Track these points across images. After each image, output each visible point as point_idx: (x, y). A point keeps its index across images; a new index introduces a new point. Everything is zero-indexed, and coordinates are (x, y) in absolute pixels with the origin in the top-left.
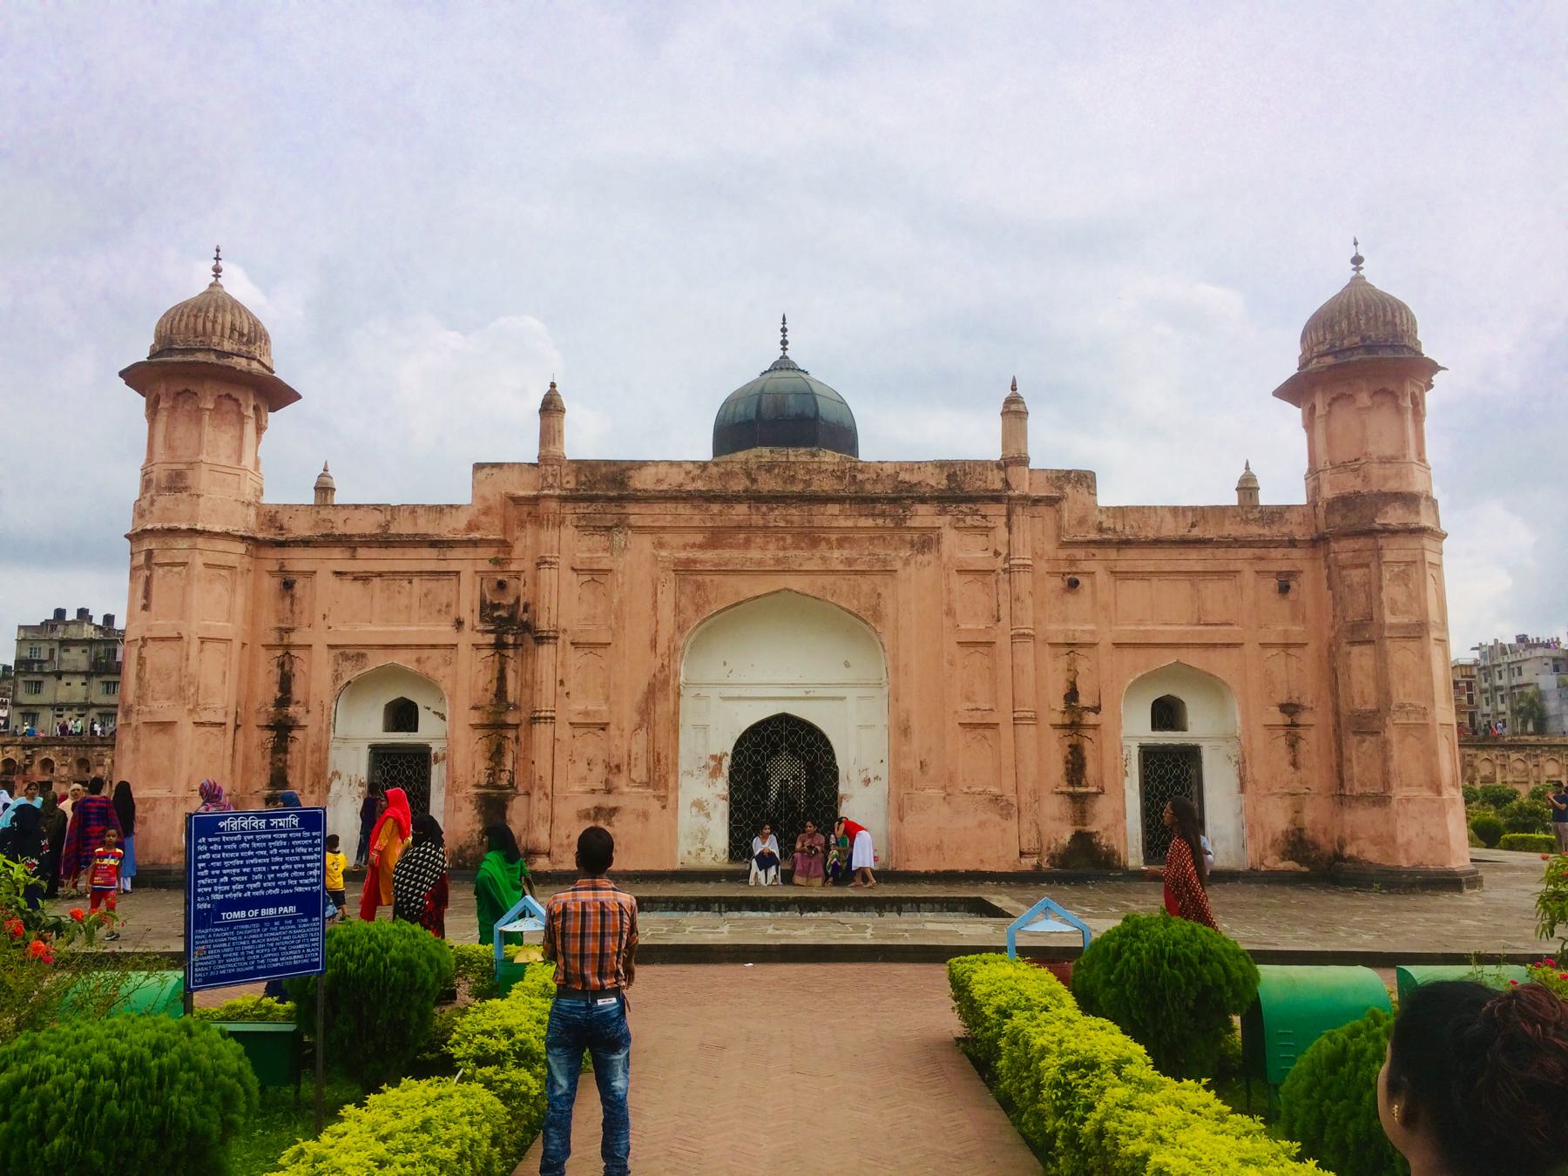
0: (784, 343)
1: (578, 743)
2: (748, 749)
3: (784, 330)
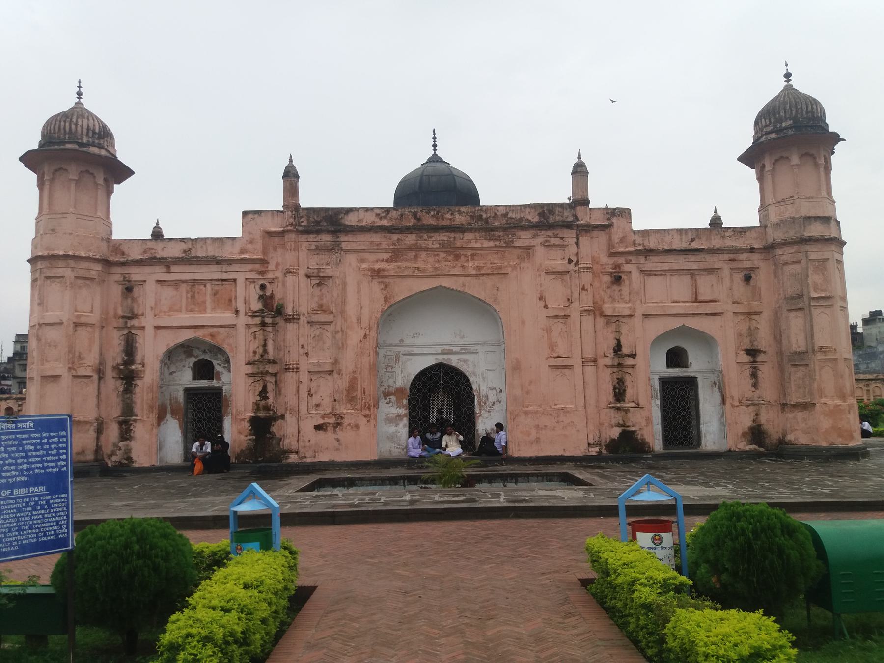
0: (435, 146)
1: (314, 384)
2: (419, 385)
3: (434, 138)
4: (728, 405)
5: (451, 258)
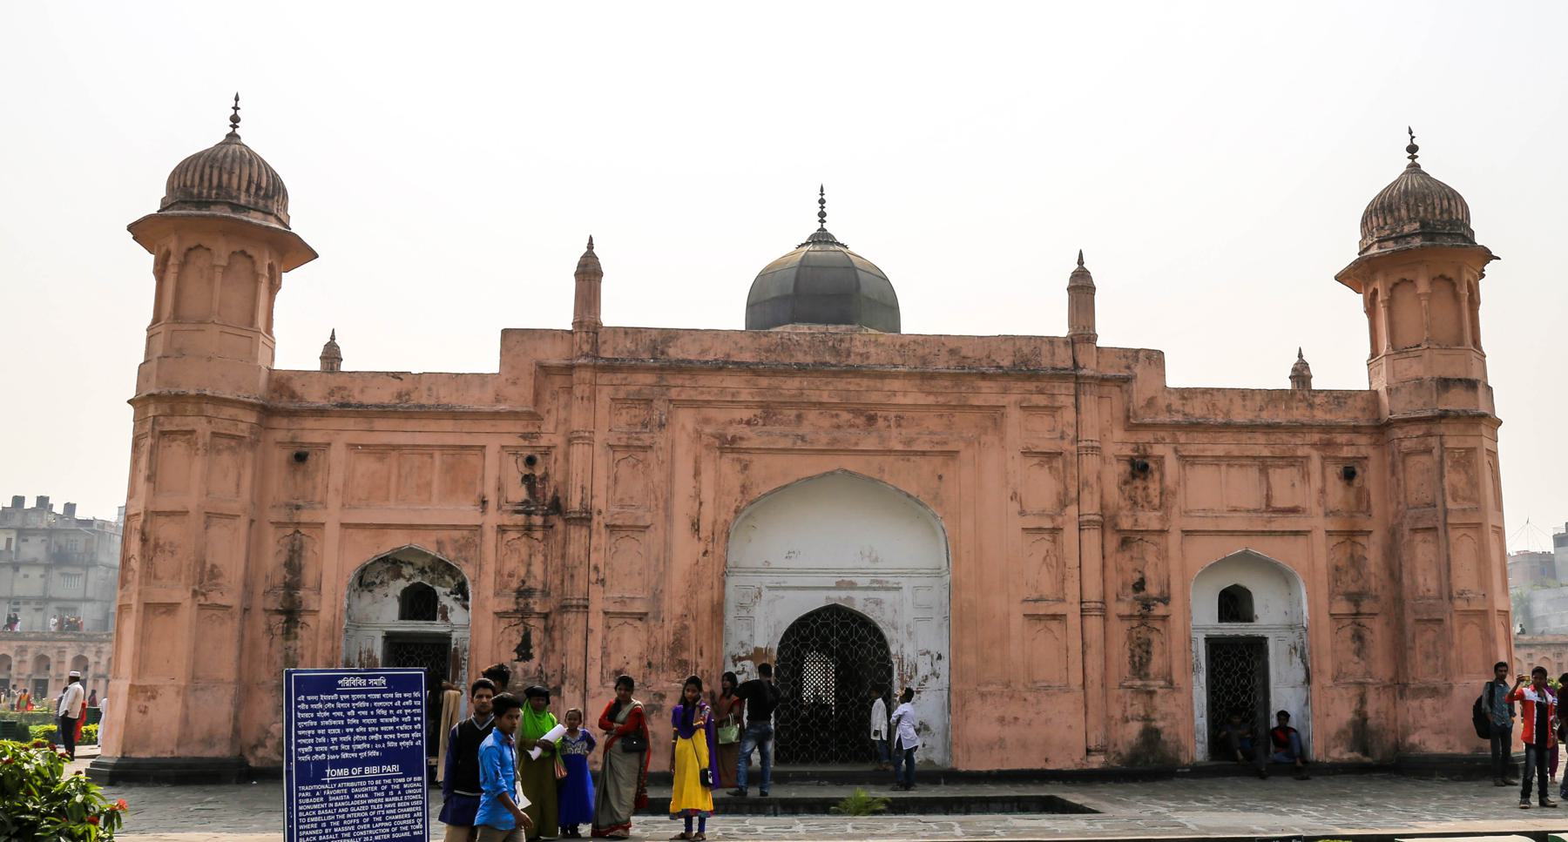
1: (612, 636)
4: (1315, 685)
5: (861, 421)
